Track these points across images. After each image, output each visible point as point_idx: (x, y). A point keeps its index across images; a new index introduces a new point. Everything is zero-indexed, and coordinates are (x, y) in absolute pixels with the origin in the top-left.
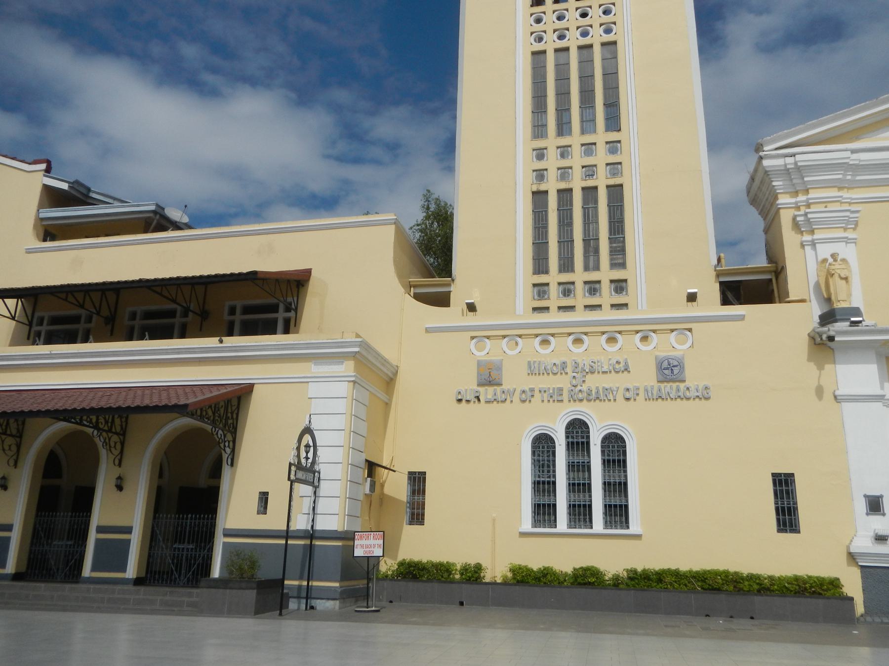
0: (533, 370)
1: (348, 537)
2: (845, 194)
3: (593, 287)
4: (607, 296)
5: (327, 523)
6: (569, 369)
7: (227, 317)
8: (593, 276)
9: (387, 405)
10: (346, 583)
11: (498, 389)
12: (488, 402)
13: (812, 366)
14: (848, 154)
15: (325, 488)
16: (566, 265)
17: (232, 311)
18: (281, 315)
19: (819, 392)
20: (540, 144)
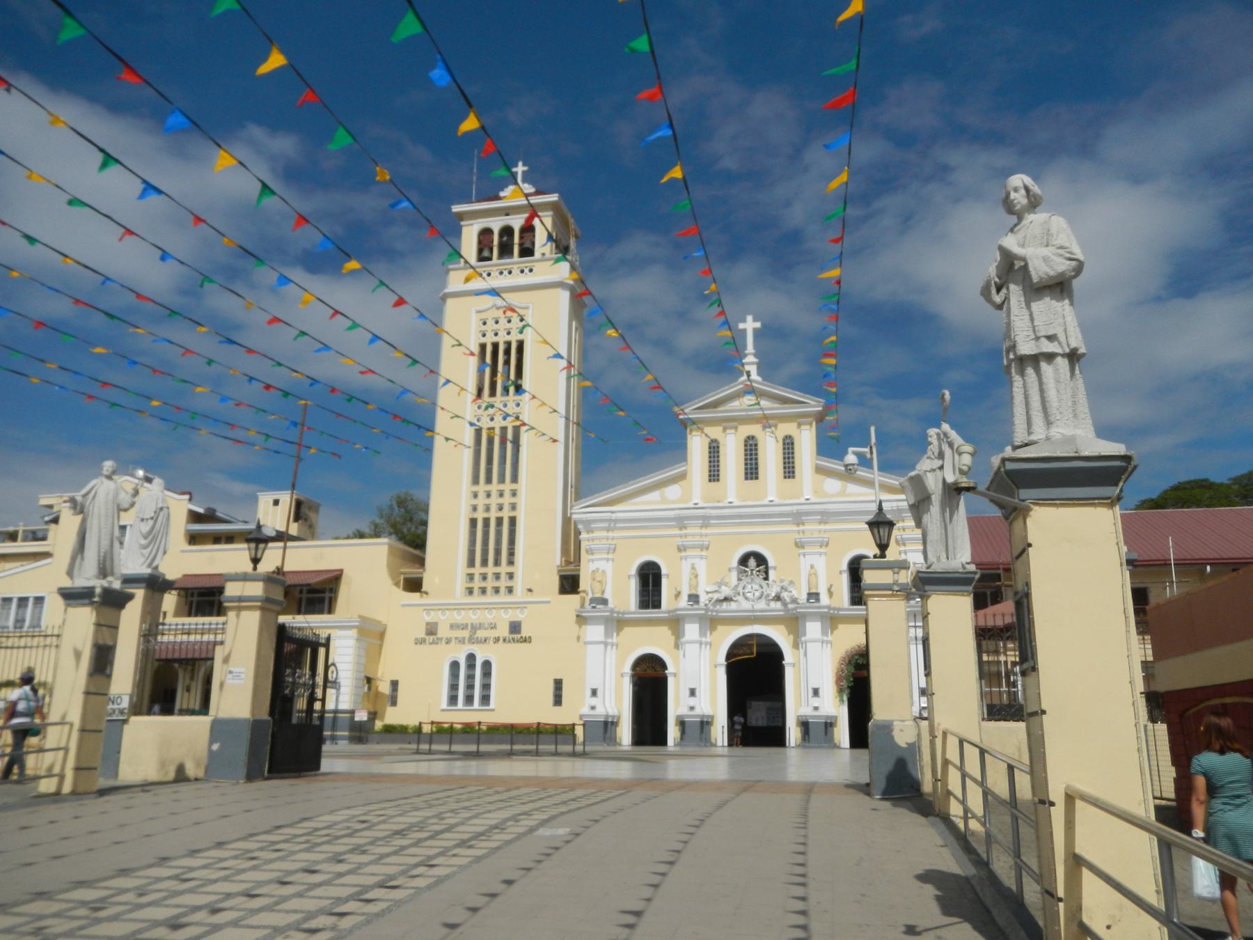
0: (453, 627)
1: (352, 712)
2: (611, 534)
3: (497, 576)
4: (503, 583)
5: (345, 705)
6: (469, 627)
7: (297, 595)
8: (497, 570)
9: (381, 646)
10: (353, 734)
11: (435, 637)
12: (431, 644)
13: (577, 626)
14: (609, 514)
15: (343, 690)
16: (484, 562)
17: (301, 592)
18: (327, 595)
19: (578, 638)
20: (475, 488)
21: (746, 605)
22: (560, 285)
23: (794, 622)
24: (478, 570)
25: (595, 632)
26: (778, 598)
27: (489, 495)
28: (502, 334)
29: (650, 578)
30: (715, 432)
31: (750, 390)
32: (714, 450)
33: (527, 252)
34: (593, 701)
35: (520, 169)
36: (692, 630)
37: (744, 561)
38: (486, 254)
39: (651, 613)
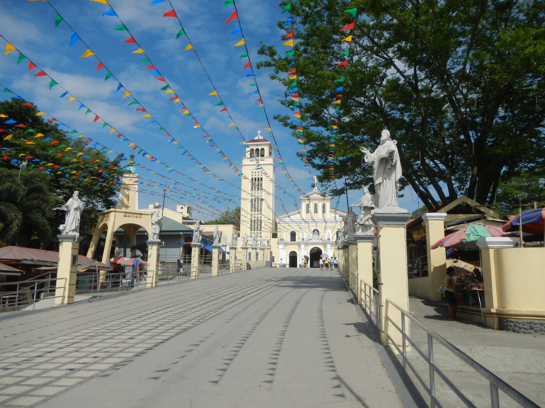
21: (314, 241)
22: (271, 164)
23: (325, 244)
24: (253, 232)
25: (281, 246)
26: (321, 239)
27: (255, 214)
28: (257, 175)
29: (293, 235)
30: (307, 202)
31: (315, 193)
32: (308, 206)
33: (263, 156)
34: (281, 261)
35: (259, 132)
36: (303, 246)
37: (314, 231)
38: (252, 155)
39: (293, 242)
